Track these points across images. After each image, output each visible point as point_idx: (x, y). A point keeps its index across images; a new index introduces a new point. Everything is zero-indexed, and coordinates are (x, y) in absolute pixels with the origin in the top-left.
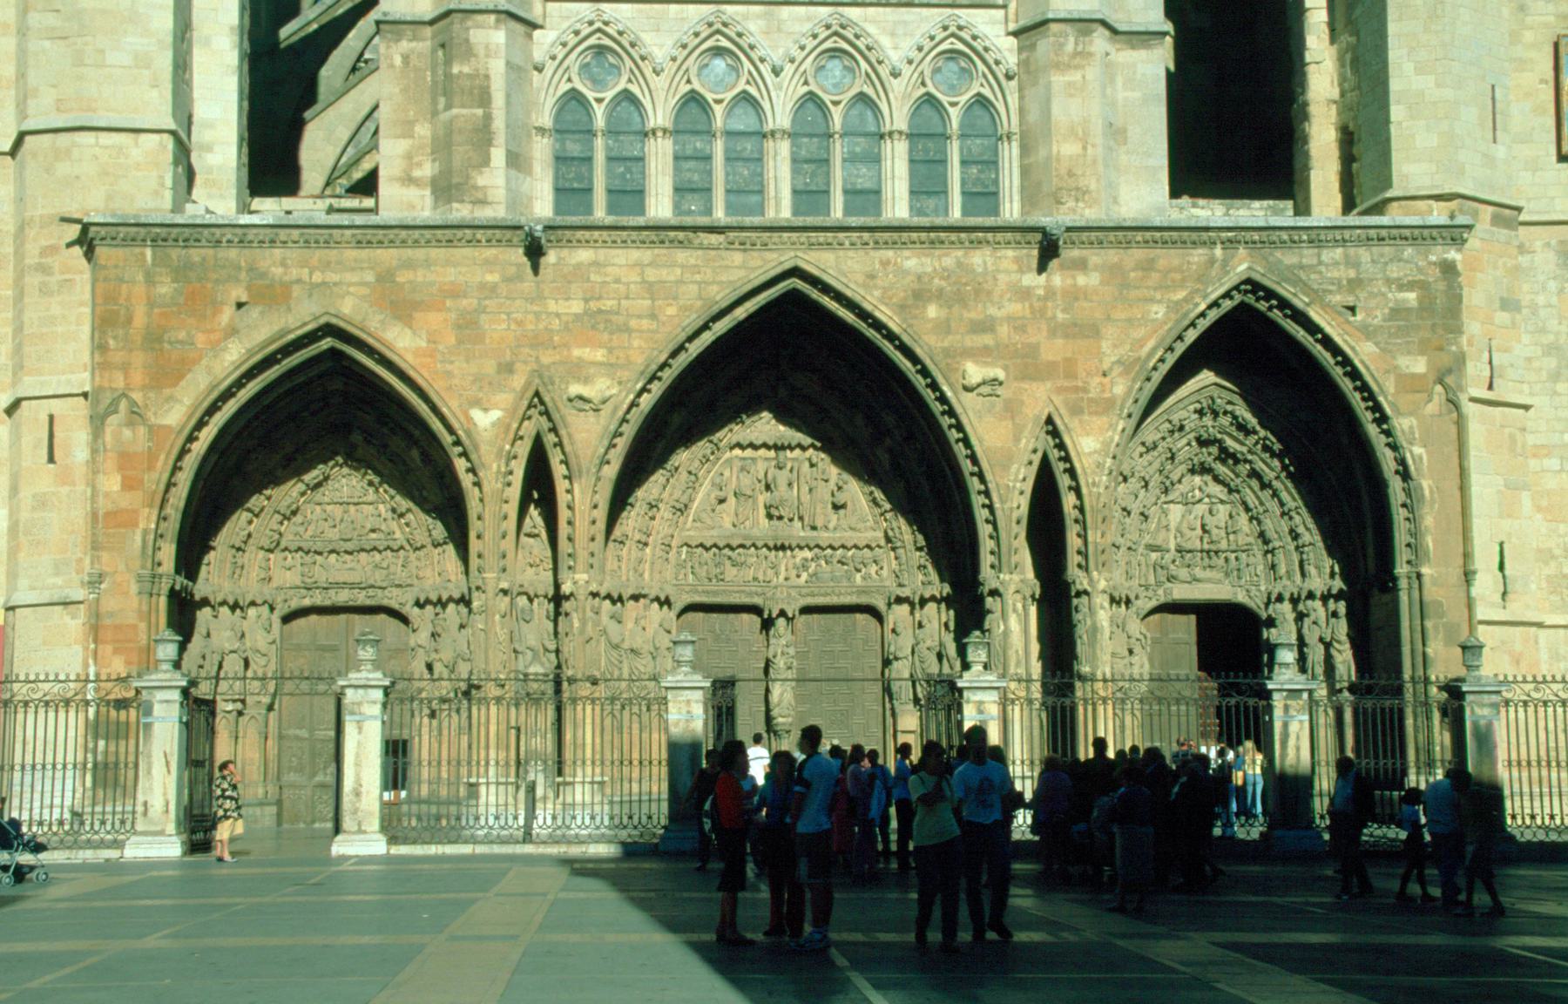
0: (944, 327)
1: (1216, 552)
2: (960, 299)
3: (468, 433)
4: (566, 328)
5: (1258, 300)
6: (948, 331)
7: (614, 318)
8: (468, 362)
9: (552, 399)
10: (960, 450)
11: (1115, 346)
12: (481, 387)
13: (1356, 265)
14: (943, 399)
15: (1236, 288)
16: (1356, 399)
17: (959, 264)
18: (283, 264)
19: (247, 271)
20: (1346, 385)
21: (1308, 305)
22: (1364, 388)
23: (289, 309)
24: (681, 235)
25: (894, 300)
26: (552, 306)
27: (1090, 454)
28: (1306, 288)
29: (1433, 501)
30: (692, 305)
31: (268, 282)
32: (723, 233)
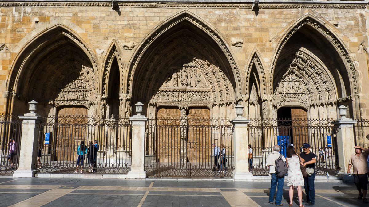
0: (226, 29)
1: (296, 94)
2: (231, 22)
3: (95, 56)
4: (123, 28)
5: (311, 23)
6: (227, 30)
7: (136, 26)
8: (96, 37)
9: (118, 47)
10: (231, 62)
11: (273, 34)
12: (99, 43)
13: (337, 14)
14: (226, 48)
15: (305, 19)
16: (338, 50)
17: (230, 12)
18: (48, 12)
19: (39, 13)
20: (336, 46)
21: (325, 24)
22: (341, 46)
23: (49, 23)
24: (154, 4)
25: (212, 22)
26: (119, 22)
27: (267, 62)
28: (324, 19)
29: (361, 76)
30: (157, 23)
31: (44, 16)
32: (166, 4)
